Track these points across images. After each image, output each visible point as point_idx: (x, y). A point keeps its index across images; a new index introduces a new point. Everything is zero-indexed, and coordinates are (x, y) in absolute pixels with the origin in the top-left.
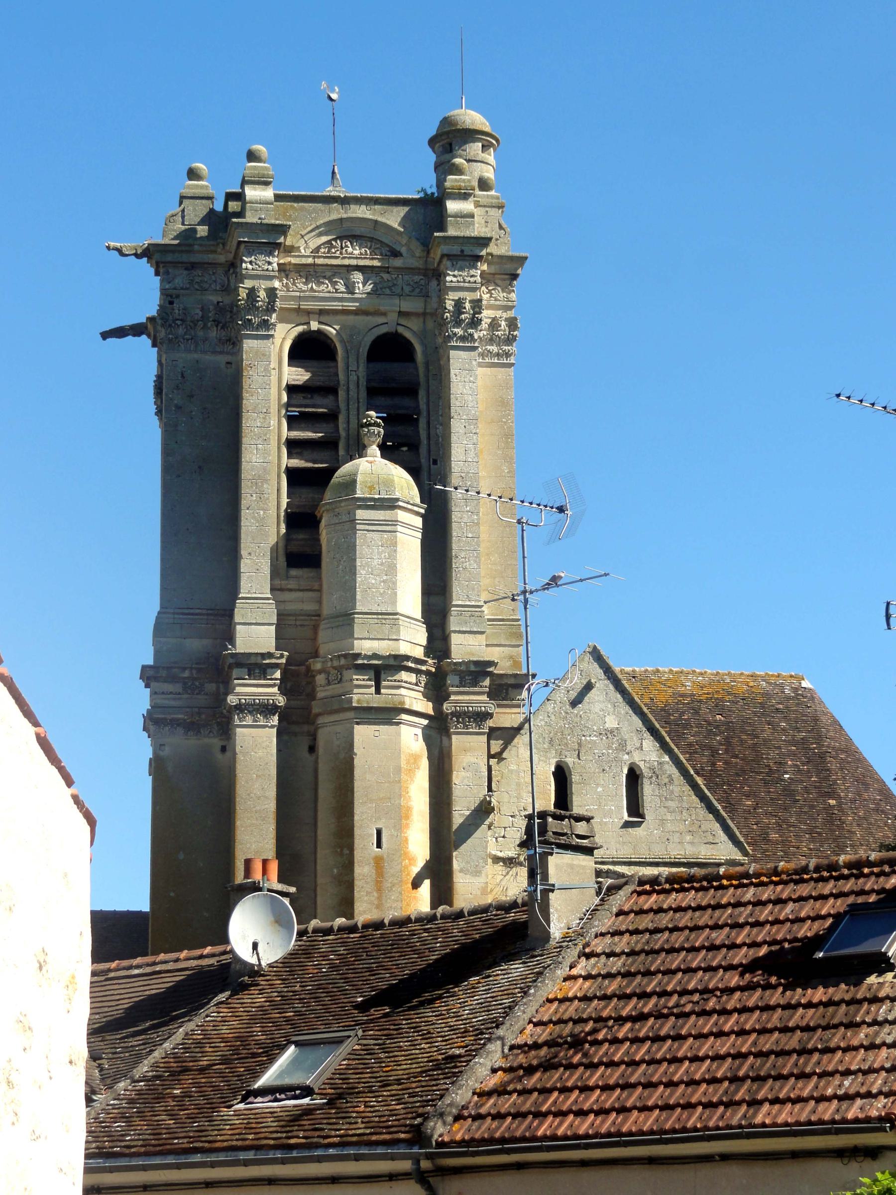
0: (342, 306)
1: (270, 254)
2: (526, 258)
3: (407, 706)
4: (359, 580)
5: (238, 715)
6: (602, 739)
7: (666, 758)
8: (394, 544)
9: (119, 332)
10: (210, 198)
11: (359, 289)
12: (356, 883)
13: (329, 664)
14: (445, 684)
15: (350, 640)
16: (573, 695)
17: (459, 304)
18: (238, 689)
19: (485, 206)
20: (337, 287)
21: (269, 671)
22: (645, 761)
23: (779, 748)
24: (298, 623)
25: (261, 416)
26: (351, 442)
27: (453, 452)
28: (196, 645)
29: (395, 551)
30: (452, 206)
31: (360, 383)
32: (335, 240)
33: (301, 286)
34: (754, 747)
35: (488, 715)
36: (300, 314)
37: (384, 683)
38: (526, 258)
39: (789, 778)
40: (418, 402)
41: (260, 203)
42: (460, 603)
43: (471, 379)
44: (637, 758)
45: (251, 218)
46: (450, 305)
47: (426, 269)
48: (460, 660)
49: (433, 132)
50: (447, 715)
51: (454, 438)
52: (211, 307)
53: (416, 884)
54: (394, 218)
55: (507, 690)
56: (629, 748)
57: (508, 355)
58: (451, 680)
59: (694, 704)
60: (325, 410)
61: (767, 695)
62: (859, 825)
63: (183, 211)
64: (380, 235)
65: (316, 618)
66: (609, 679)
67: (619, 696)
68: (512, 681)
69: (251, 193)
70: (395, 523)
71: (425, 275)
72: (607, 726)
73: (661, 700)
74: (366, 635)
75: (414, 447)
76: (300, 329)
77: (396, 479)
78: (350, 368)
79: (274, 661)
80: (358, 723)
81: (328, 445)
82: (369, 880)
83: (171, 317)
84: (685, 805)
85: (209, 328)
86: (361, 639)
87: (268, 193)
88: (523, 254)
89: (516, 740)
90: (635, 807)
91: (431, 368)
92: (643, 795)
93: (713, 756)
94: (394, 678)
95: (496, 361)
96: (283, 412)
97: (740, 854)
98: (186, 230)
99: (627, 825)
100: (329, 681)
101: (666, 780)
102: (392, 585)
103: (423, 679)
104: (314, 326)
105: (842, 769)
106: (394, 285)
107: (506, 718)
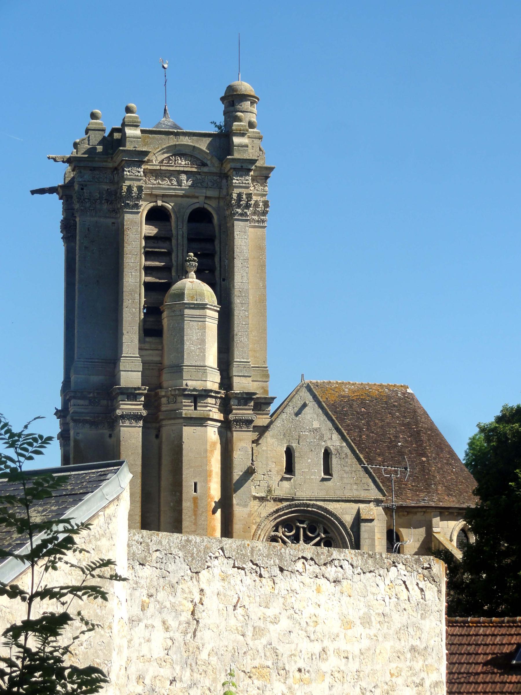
0: (175, 193)
1: (140, 166)
2: (274, 168)
3: (211, 417)
4: (185, 347)
5: (122, 420)
6: (311, 434)
7: (344, 444)
8: (204, 328)
9: (42, 191)
10: (104, 130)
11: (184, 184)
12: (183, 511)
13: (169, 393)
14: (229, 404)
15: (180, 380)
16: (296, 409)
17: (239, 195)
18: (122, 406)
19: (252, 138)
20: (172, 182)
21: (138, 396)
22: (333, 445)
23: (395, 427)
24: (150, 368)
25: (134, 256)
27: (235, 277)
28: (96, 379)
29: (205, 332)
30: (236, 140)
31: (184, 235)
32: (172, 156)
33: (153, 181)
34: (382, 427)
35: (251, 421)
36: (153, 197)
37: (199, 404)
38: (274, 168)
39: (401, 445)
40: (214, 246)
41: (134, 138)
42: (238, 360)
43: (246, 237)
44: (329, 444)
45: (129, 147)
46: (235, 196)
47: (221, 173)
48: (239, 392)
49: (223, 95)
50: (231, 421)
51: (236, 269)
52: (104, 192)
53: (214, 512)
54: (203, 145)
55: (260, 406)
56: (325, 439)
57: (263, 221)
59: (350, 402)
60: (166, 250)
61: (388, 397)
62: (438, 472)
63: (89, 137)
65: (160, 365)
66: (315, 401)
67: (320, 410)
68: (263, 401)
69: (129, 131)
70: (205, 316)
71: (220, 177)
72: (314, 426)
73: (332, 399)
74: (189, 378)
75: (212, 271)
76: (152, 205)
77: (205, 292)
78: (179, 227)
79: (141, 392)
80: (185, 426)
81: (167, 269)
82: (190, 510)
83: (82, 198)
84: (353, 469)
85: (103, 204)
86: (187, 380)
87: (137, 132)
88: (273, 166)
89: (266, 434)
90: (327, 470)
91: (222, 228)
92: (332, 464)
93: (360, 432)
95: (257, 225)
96: (143, 251)
97: (381, 495)
98: (91, 148)
99: (323, 480)
100: (169, 402)
101: (344, 456)
102: (203, 350)
103: (218, 401)
104: (160, 203)
105: (429, 440)
106: (203, 182)
107: (261, 420)
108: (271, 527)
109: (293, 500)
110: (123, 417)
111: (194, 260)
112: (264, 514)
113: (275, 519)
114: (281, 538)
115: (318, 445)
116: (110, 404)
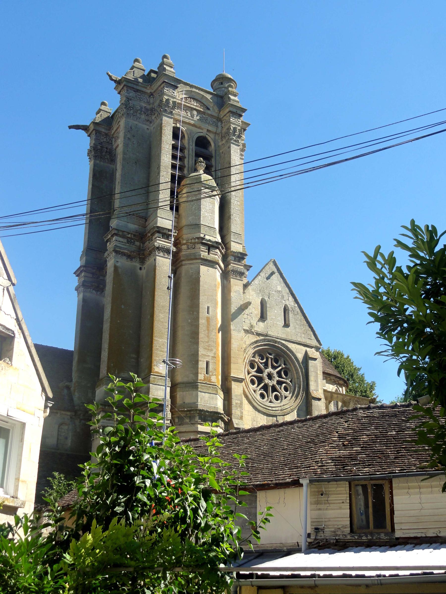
2: (250, 124)
4: (202, 213)
7: (296, 305)
9: (77, 127)
10: (144, 70)
12: (200, 325)
16: (267, 275)
26: (189, 169)
28: (132, 227)
32: (188, 98)
38: (250, 124)
44: (287, 303)
47: (218, 117)
53: (219, 332)
56: (285, 299)
58: (231, 258)
64: (203, 101)
80: (202, 265)
94: (215, 251)
100: (188, 248)
101: (296, 313)
108: (252, 353)
109: (267, 336)
110: (158, 248)
111: (203, 163)
112: (248, 343)
113: (254, 348)
114: (256, 362)
115: (281, 302)
116: (142, 246)
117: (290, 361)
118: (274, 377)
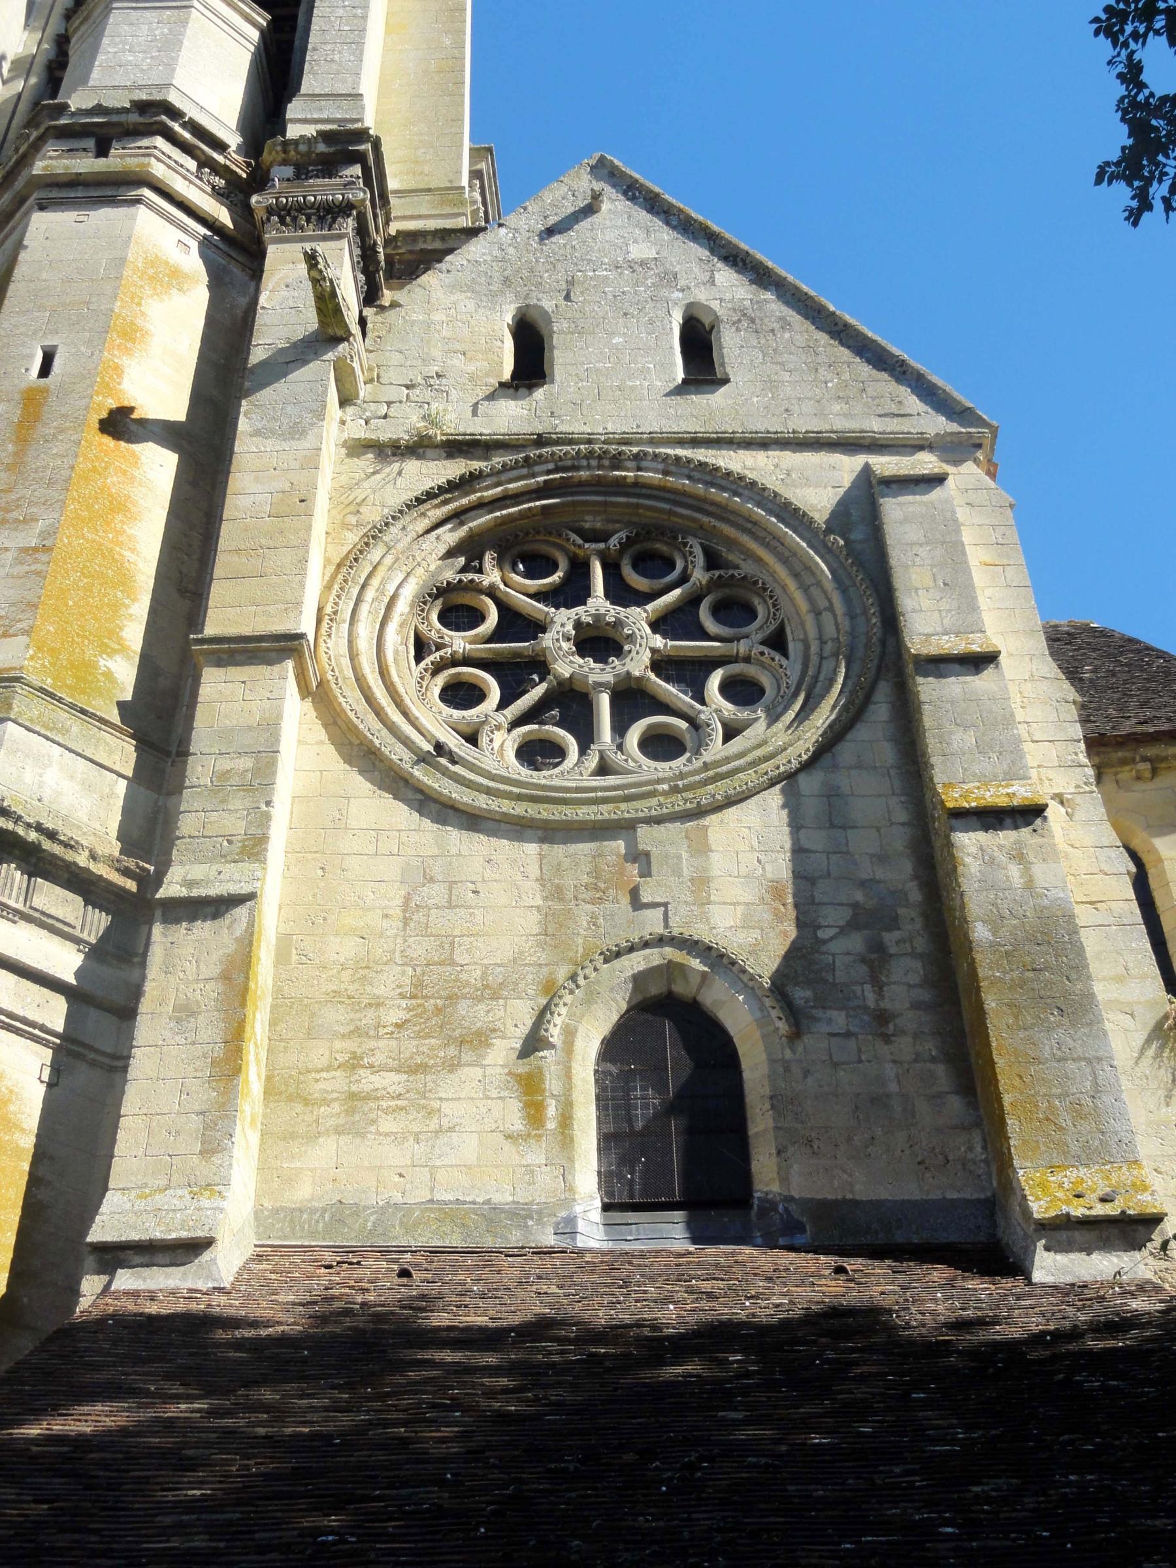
22: (721, 300)
44: (702, 295)
56: (682, 283)
72: (632, 256)
114: (492, 592)
117: (745, 539)
118: (618, 624)
